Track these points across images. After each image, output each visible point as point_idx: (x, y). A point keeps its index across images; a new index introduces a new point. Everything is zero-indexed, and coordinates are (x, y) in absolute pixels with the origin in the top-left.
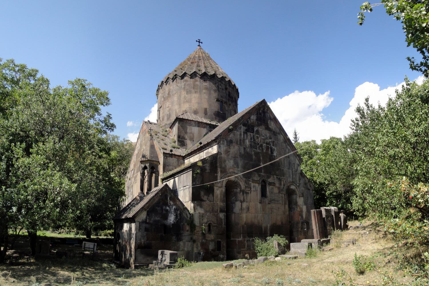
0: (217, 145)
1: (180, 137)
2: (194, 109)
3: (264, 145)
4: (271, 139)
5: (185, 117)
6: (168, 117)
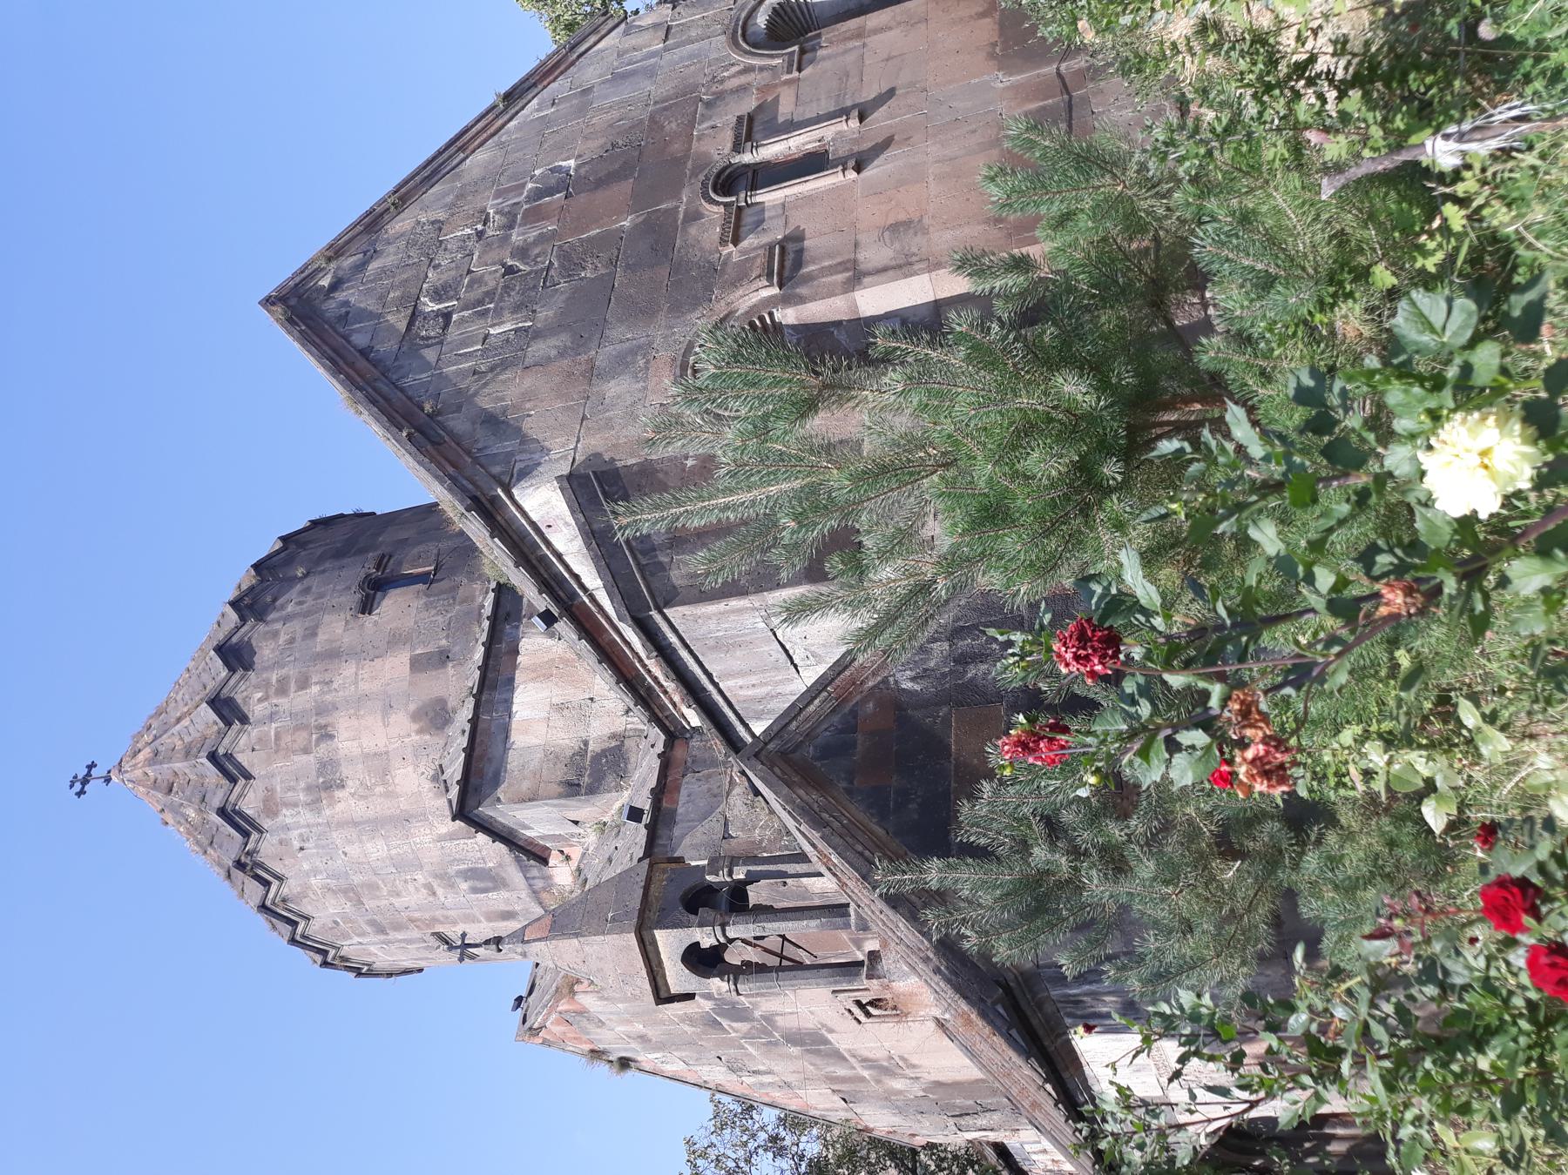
0: (515, 491)
1: (570, 784)
2: (420, 731)
3: (516, 237)
4: (483, 211)
5: (455, 771)
6: (490, 885)
